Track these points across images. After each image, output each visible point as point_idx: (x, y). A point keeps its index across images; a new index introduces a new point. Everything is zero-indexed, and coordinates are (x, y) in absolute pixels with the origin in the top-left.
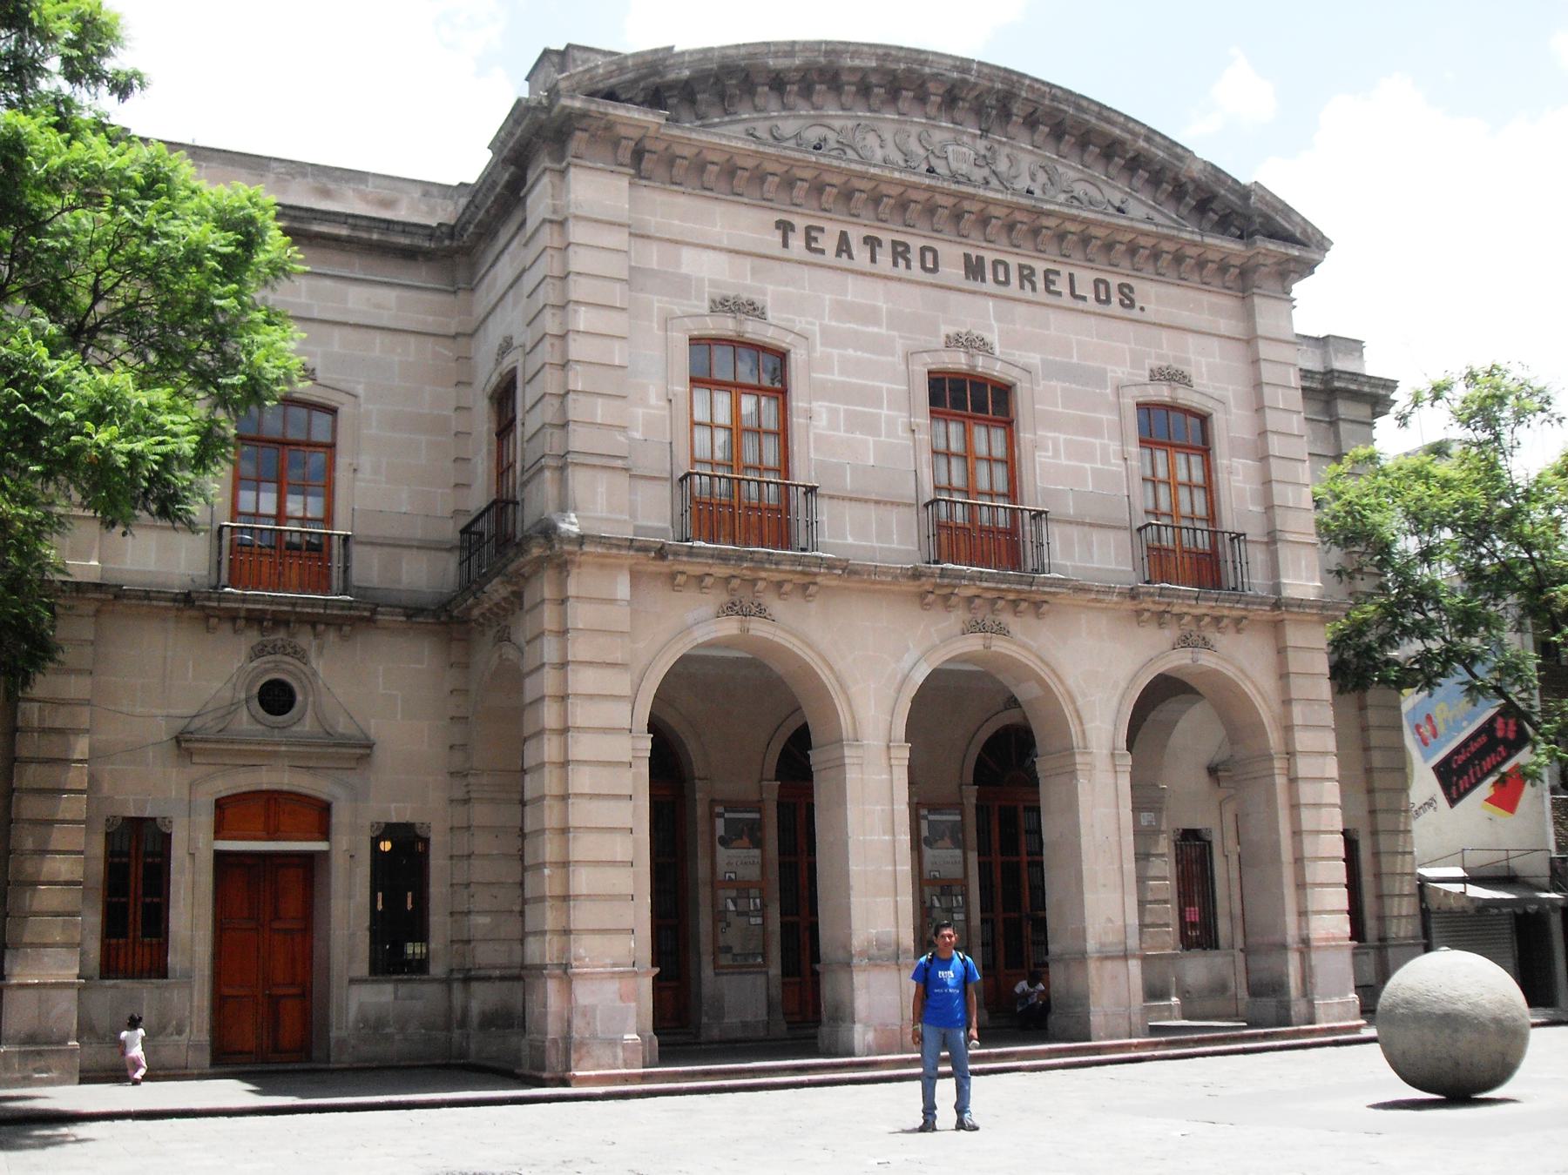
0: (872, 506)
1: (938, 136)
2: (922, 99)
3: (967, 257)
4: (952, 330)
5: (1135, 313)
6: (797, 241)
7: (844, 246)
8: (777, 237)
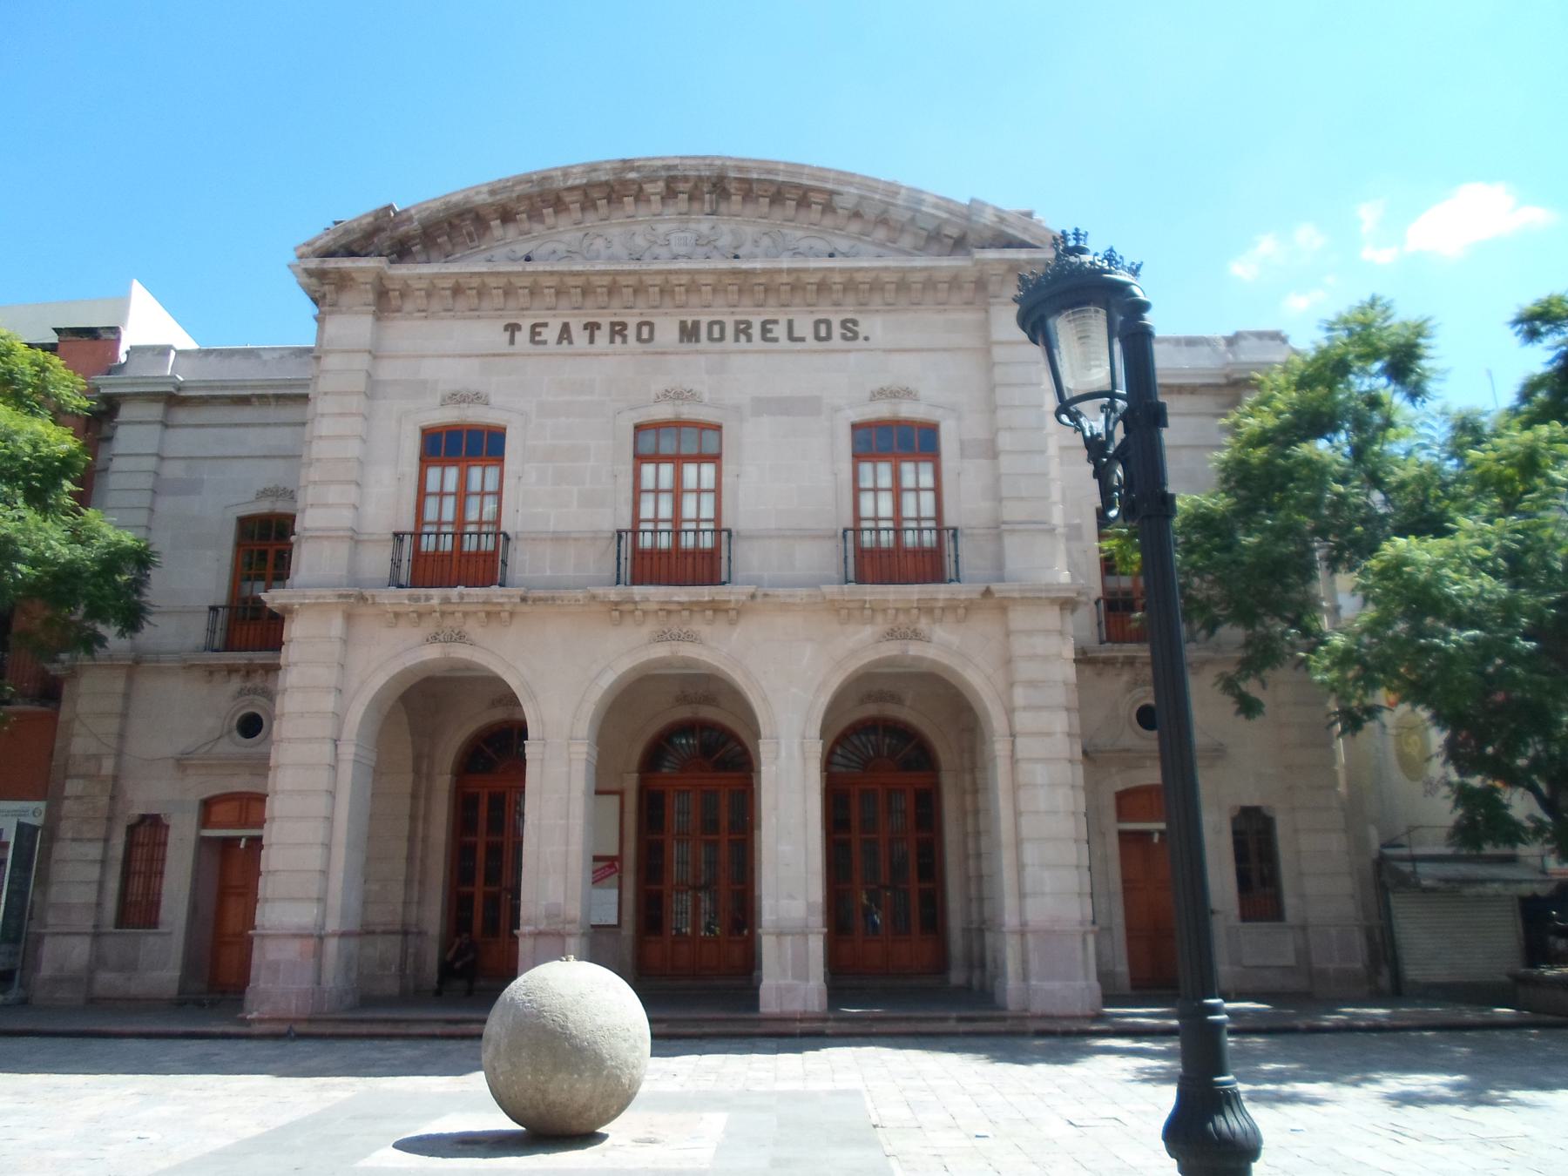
1: (662, 228)
2: (640, 197)
5: (860, 343)
6: (523, 337)
7: (565, 332)
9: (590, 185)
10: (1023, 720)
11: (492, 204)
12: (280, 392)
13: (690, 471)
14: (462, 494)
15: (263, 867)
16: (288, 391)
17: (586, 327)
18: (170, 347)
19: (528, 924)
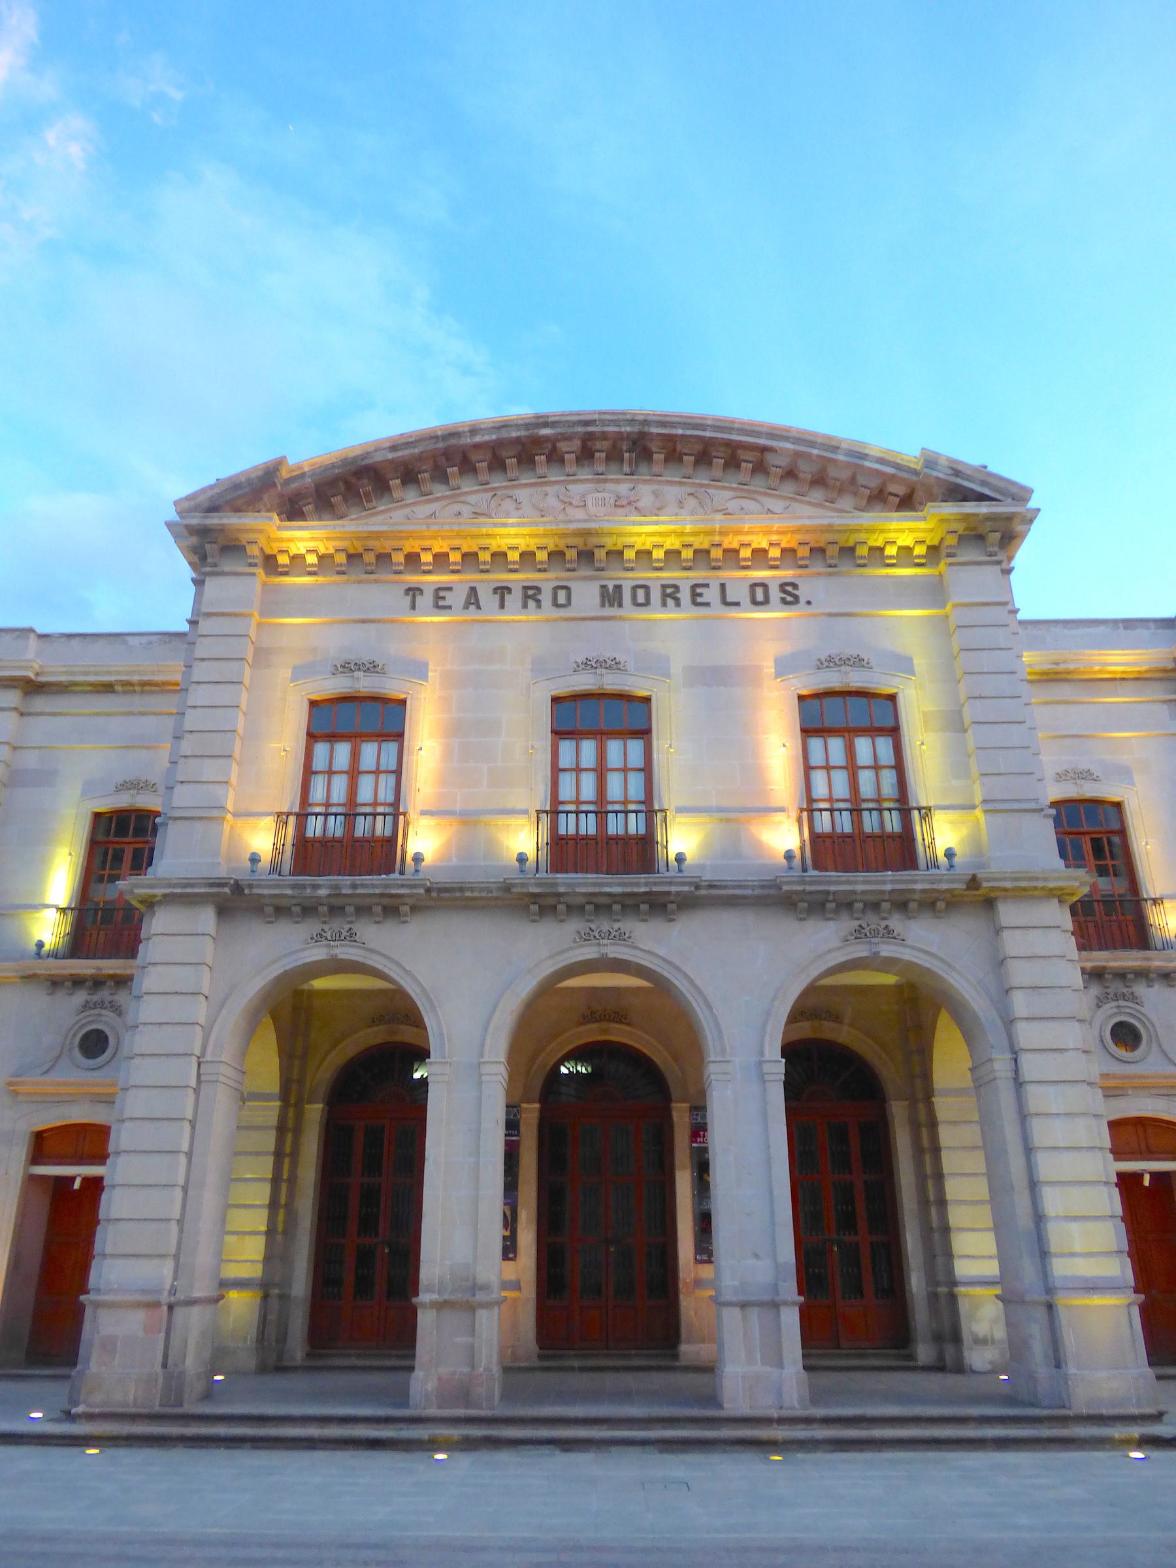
2: (555, 458)
3: (603, 587)
4: (581, 659)
7: (473, 599)
8: (409, 599)
10: (1027, 1035)
11: (391, 461)
12: (145, 678)
13: (614, 748)
14: (354, 773)
15: (102, 1214)
17: (495, 590)
18: (32, 630)
19: (430, 1290)
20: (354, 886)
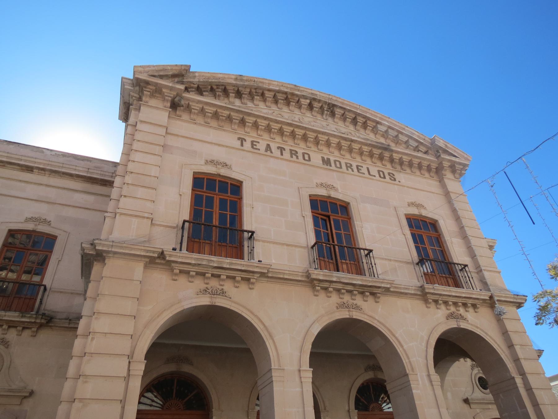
0: (285, 247)
2: (299, 106)
4: (319, 182)
6: (247, 145)
8: (239, 142)
9: (279, 92)
16: (60, 170)
20: (231, 264)
